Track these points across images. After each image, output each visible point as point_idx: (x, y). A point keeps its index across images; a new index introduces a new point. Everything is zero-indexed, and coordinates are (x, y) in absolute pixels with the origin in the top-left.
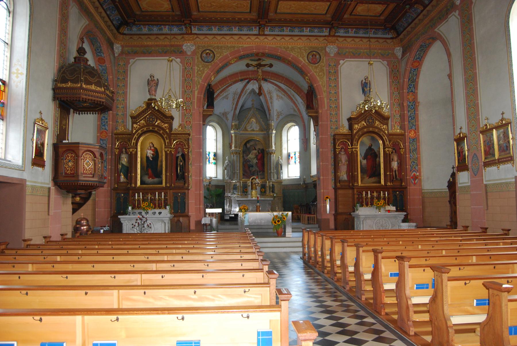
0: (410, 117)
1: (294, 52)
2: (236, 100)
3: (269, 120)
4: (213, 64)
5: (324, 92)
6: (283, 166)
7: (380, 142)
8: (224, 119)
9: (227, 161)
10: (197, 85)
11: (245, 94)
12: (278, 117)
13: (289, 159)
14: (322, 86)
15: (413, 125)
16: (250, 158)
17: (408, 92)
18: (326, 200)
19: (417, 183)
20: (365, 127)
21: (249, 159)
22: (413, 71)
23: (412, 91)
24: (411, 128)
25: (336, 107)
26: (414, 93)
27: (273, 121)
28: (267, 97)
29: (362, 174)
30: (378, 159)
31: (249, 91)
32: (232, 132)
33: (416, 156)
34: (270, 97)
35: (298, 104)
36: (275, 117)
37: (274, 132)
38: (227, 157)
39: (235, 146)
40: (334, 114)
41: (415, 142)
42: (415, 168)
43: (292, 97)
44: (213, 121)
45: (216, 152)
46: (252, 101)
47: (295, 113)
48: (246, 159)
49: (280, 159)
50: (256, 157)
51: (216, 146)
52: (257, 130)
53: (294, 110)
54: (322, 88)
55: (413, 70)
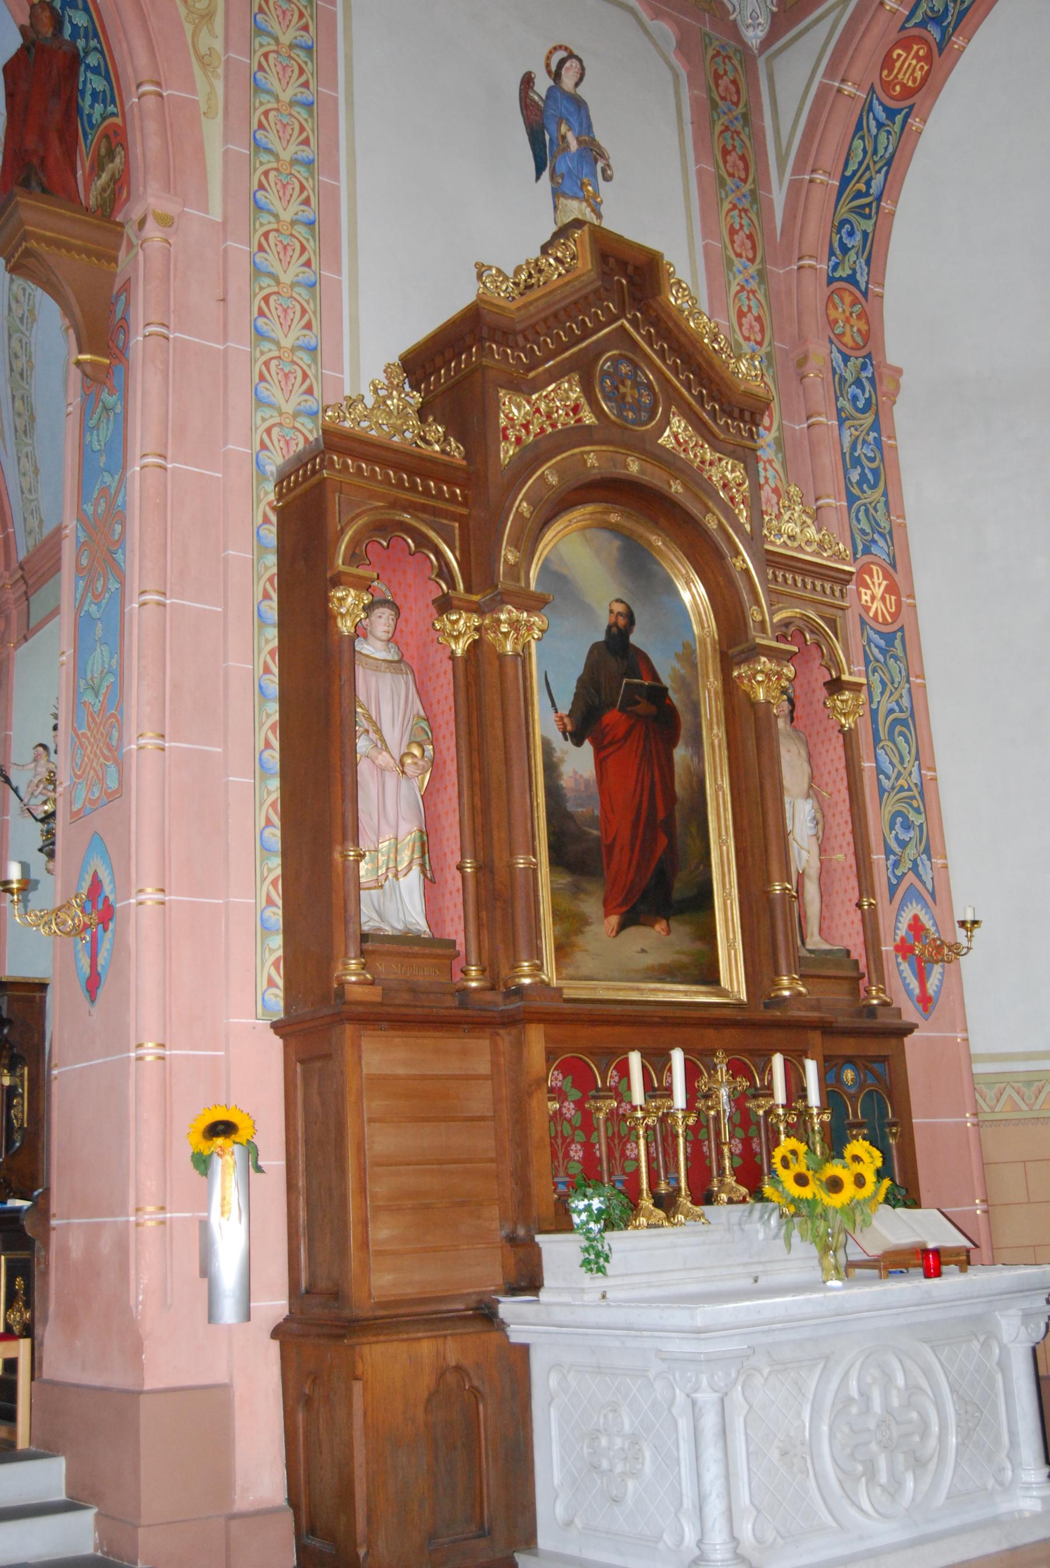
0: (854, 467)
5: (204, 65)
7: (686, 596)
14: (183, 11)
15: (875, 526)
17: (831, 280)
18: (202, 1163)
19: (938, 992)
20: (580, 435)
22: (880, 125)
23: (852, 279)
24: (867, 551)
25: (310, 224)
26: (865, 294)
29: (565, 880)
30: (680, 753)
33: (915, 770)
40: (286, 278)
41: (896, 658)
42: (915, 869)
54: (189, 29)
55: (882, 116)
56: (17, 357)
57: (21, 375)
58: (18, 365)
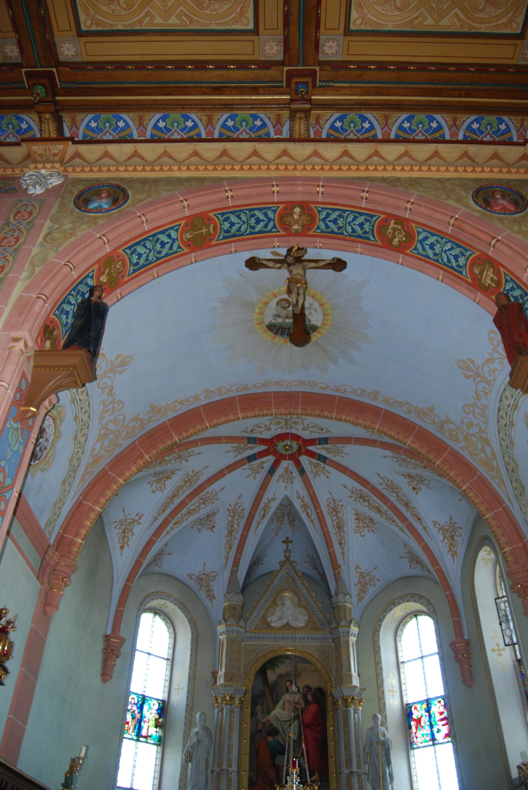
1: (421, 189)
2: (238, 535)
3: (337, 594)
4: (114, 215)
6: (392, 752)
8: (203, 595)
9: (196, 729)
10: (34, 266)
11: (264, 515)
12: (363, 590)
13: (410, 727)
16: (276, 717)
21: (276, 724)
27: (348, 597)
28: (326, 526)
31: (274, 505)
32: (221, 628)
34: (338, 523)
35: (425, 529)
36: (354, 590)
37: (354, 630)
38: (198, 715)
39: (226, 674)
43: (403, 509)
44: (168, 597)
45: (166, 700)
46: (284, 542)
47: (417, 571)
48: (264, 724)
49: (379, 723)
50: (296, 718)
51: (168, 678)
52: (302, 625)
53: (414, 559)
56: (508, 464)
57: (513, 471)
58: (510, 468)
